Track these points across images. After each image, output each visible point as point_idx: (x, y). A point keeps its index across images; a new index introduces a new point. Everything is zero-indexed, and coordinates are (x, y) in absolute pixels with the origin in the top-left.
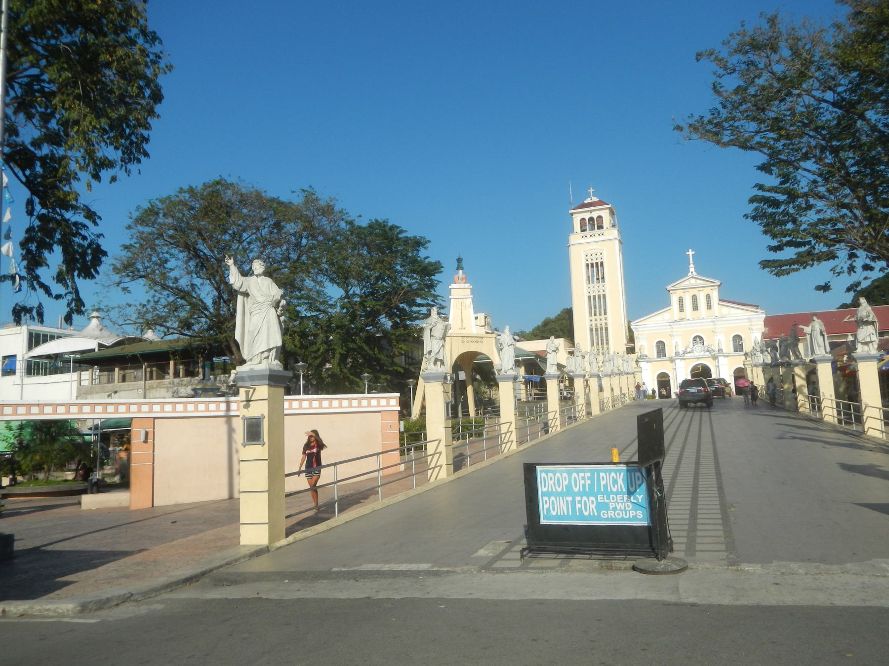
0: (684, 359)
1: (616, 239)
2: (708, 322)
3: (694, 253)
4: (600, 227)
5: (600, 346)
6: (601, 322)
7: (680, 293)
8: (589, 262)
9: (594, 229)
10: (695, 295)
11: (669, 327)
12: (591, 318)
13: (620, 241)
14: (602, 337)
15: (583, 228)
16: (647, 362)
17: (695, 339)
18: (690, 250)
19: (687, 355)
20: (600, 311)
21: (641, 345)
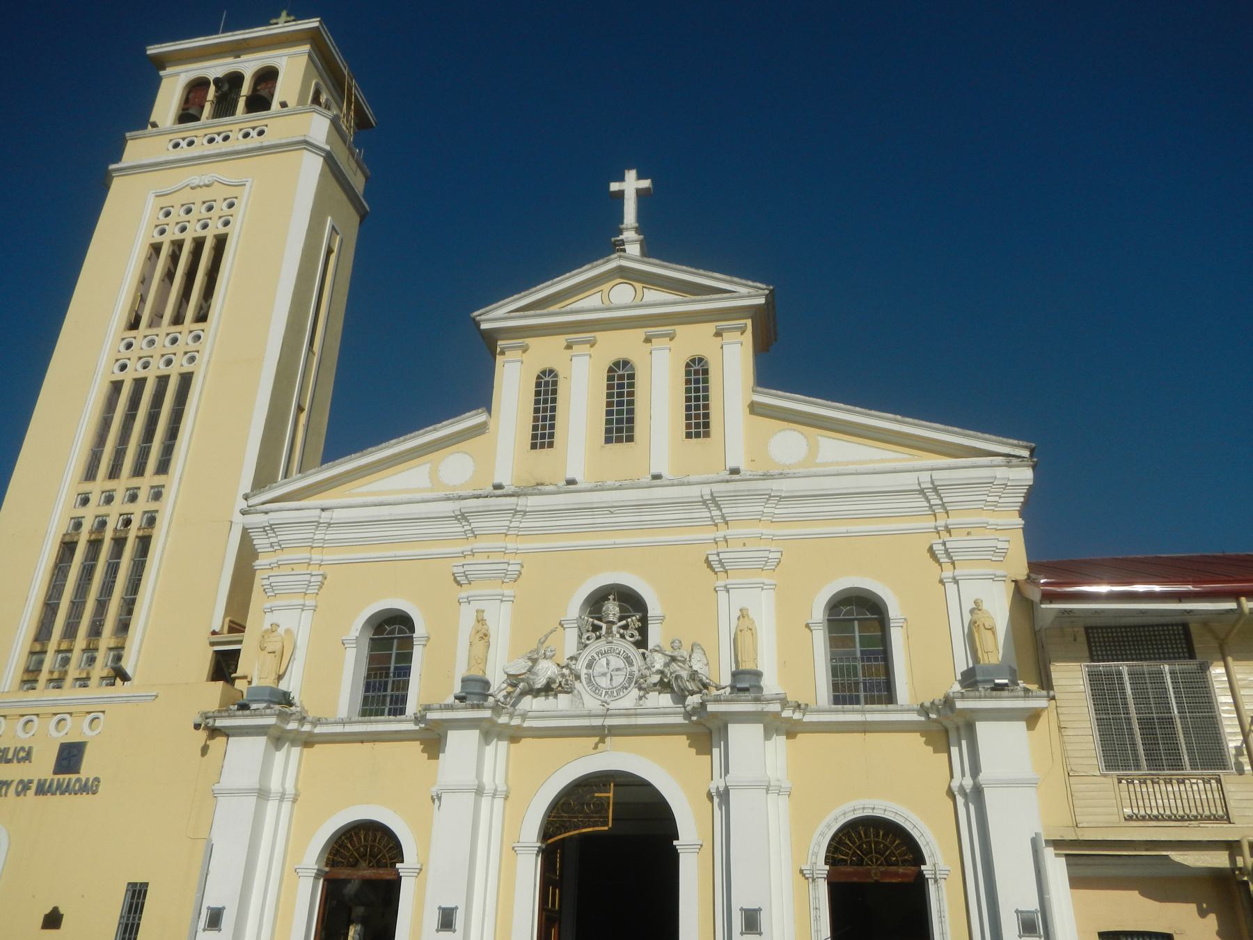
0: (515, 736)
1: (306, 144)
2: (688, 503)
3: (646, 183)
4: (259, 103)
5: (81, 641)
6: (129, 508)
7: (545, 352)
8: (173, 234)
9: (233, 114)
10: (626, 363)
11: (456, 528)
12: (88, 487)
13: (329, 159)
14: (107, 589)
15: (192, 111)
16: (278, 739)
17: (596, 602)
18: (631, 175)
19: (528, 703)
20: (143, 455)
21: (275, 626)
